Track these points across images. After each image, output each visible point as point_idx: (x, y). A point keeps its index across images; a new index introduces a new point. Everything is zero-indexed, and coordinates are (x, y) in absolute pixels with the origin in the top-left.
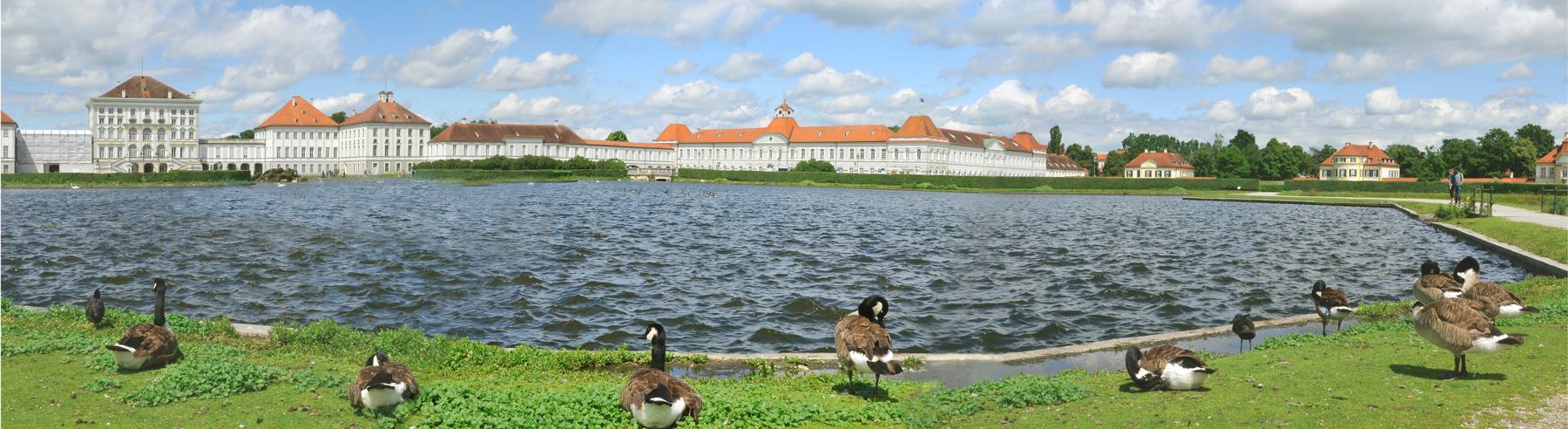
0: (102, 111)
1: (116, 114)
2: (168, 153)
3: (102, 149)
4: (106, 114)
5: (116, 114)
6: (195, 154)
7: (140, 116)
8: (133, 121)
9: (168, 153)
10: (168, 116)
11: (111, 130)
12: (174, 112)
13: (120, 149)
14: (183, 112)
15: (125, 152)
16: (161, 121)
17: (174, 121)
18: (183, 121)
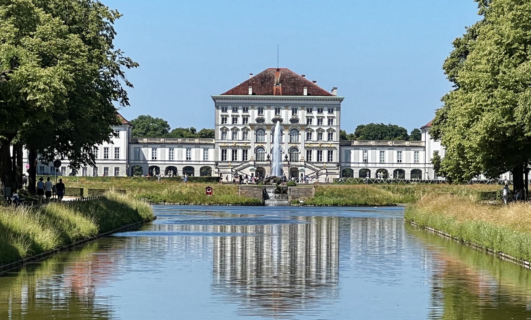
0: (224, 110)
1: (240, 112)
2: (302, 155)
3: (224, 152)
4: (230, 112)
5: (240, 112)
6: (335, 158)
8: (260, 120)
9: (302, 155)
10: (302, 115)
11: (235, 131)
12: (309, 111)
13: (245, 152)
14: (320, 111)
15: (251, 154)
16: (294, 121)
17: (309, 120)
18: (320, 120)
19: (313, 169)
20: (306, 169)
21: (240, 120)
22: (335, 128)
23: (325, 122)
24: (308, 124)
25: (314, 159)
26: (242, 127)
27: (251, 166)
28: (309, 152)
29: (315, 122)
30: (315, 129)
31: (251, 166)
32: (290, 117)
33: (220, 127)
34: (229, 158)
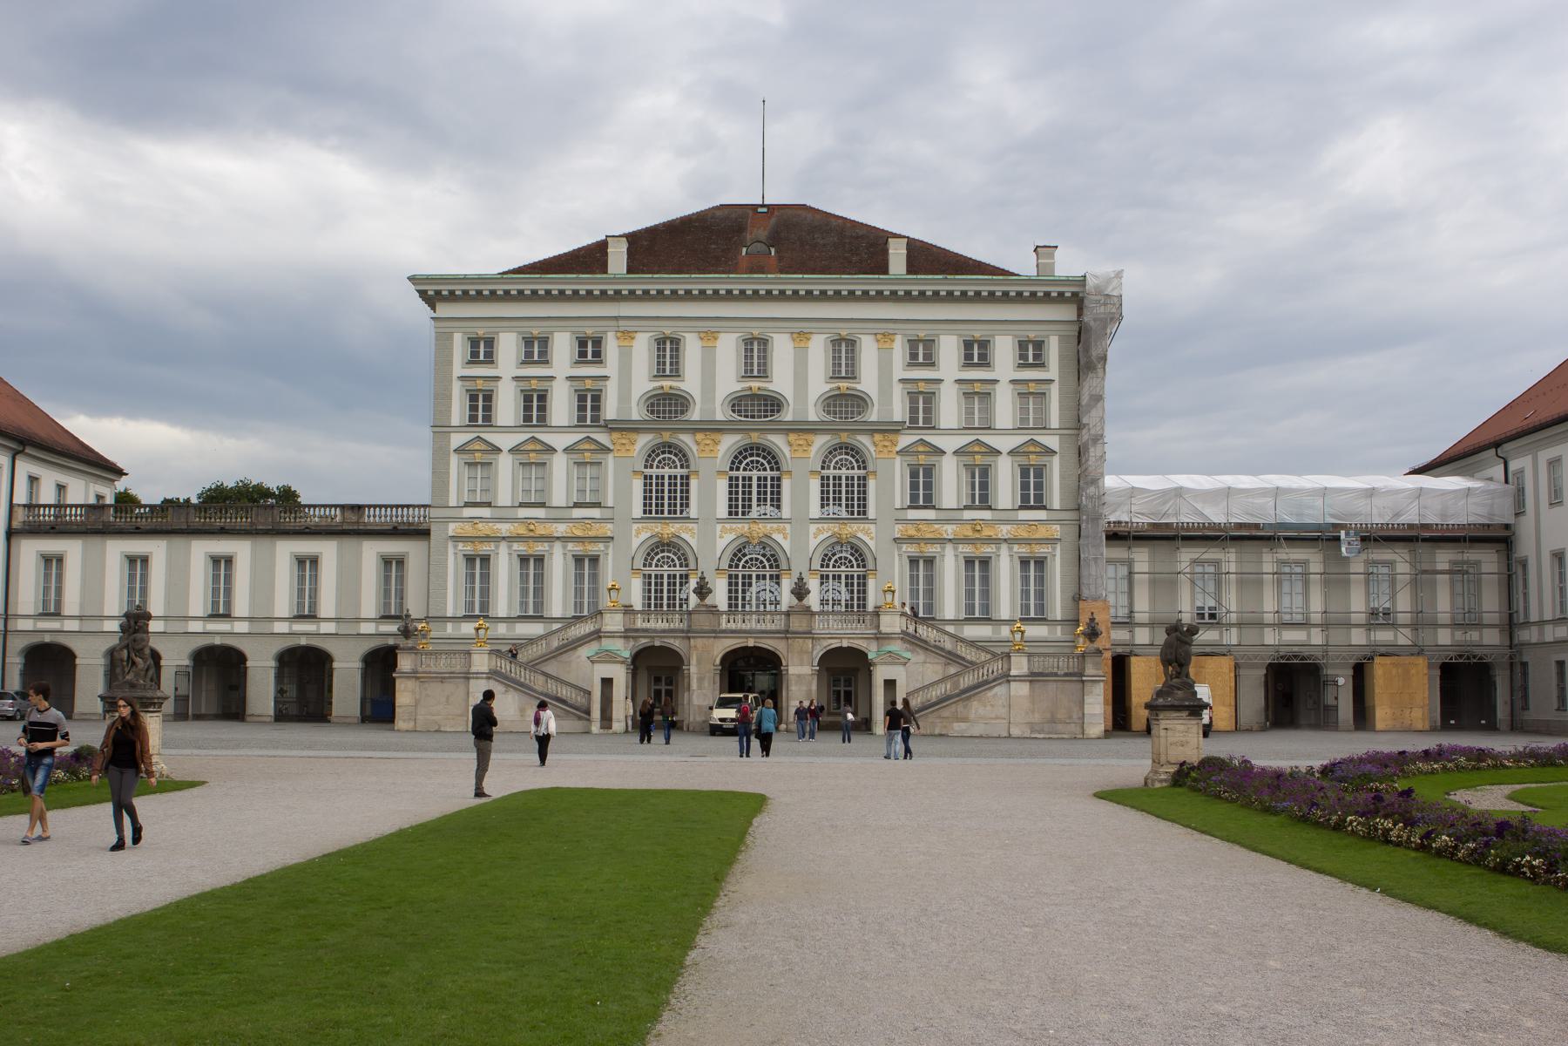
3: (479, 564)
7: (713, 376)
8: (667, 406)
11: (534, 458)
12: (922, 352)
13: (587, 563)
16: (845, 403)
17: (922, 402)
19: (951, 657)
20: (917, 657)
21: (561, 407)
22: (1052, 442)
23: (1005, 408)
24: (914, 420)
25: (949, 606)
27: (612, 635)
28: (922, 566)
29: (949, 409)
30: (949, 443)
31: (612, 635)
32: (819, 384)
33: (457, 440)
34: (503, 603)
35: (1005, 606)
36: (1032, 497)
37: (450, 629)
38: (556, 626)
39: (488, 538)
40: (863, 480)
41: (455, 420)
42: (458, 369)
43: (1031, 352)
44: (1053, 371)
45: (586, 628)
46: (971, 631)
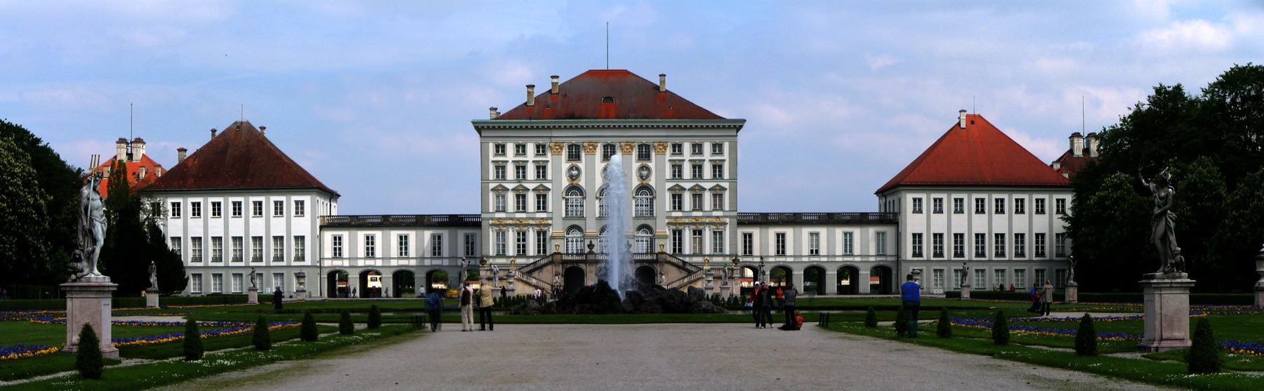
22: (726, 185)
23: (707, 171)
25: (687, 249)
26: (535, 185)
33: (492, 186)
35: (708, 249)
36: (718, 205)
37: (491, 261)
38: (532, 261)
39: (506, 225)
40: (652, 200)
41: (491, 178)
42: (492, 158)
43: (717, 148)
44: (726, 156)
45: (545, 261)
46: (695, 259)
